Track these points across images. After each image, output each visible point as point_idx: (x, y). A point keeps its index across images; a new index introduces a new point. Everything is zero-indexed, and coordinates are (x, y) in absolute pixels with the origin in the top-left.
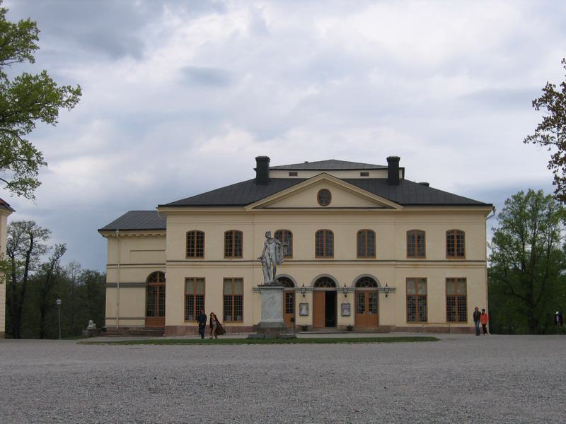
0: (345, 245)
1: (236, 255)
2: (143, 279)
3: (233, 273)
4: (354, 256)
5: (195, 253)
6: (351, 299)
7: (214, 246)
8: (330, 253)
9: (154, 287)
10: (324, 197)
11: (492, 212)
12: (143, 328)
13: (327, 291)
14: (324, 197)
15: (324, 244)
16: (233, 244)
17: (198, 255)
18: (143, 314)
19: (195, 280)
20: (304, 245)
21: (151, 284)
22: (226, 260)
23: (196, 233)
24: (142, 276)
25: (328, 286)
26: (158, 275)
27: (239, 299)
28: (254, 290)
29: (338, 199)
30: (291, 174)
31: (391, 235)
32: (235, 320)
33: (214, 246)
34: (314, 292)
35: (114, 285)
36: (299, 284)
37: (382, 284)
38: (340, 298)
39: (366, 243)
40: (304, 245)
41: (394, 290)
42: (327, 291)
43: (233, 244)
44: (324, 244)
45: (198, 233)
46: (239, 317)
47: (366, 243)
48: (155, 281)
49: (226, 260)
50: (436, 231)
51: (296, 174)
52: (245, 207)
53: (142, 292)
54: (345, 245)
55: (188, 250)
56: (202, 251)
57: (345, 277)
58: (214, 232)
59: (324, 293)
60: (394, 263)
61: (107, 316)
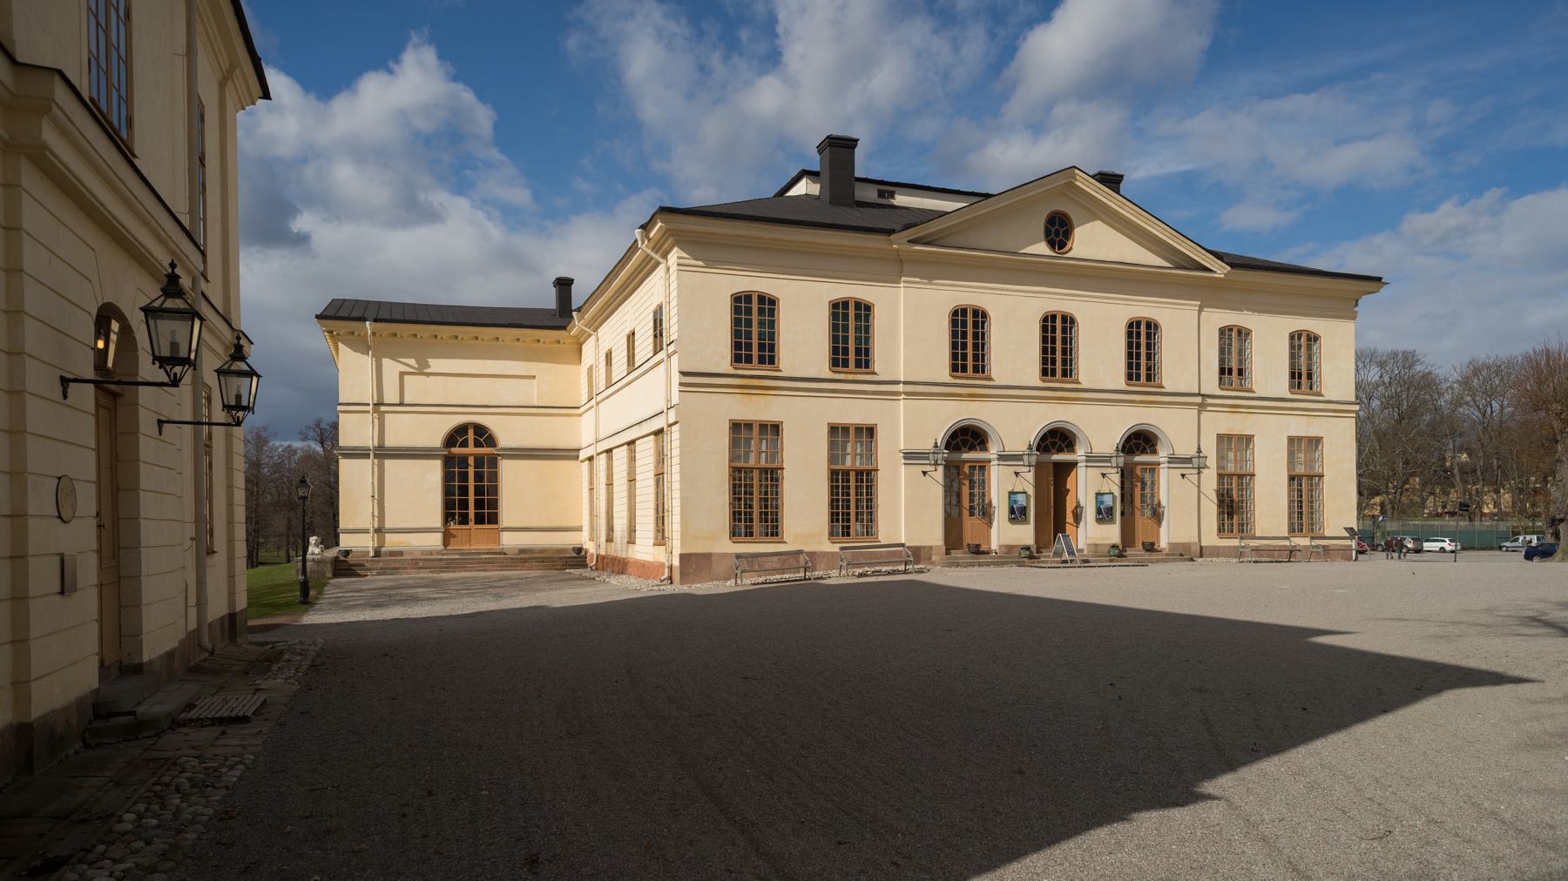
1: (858, 365)
2: (436, 440)
3: (853, 412)
5: (755, 353)
6: (1113, 484)
7: (803, 339)
9: (463, 461)
12: (439, 553)
15: (1057, 344)
16: (851, 339)
17: (762, 360)
18: (437, 522)
20: (1013, 350)
21: (456, 450)
22: (837, 376)
24: (433, 432)
26: (471, 432)
27: (866, 478)
28: (911, 456)
30: (881, 194)
33: (803, 339)
35: (358, 453)
40: (1013, 350)
44: (1057, 344)
45: (762, 298)
48: (464, 444)
51: (892, 195)
52: (893, 237)
53: (433, 472)
55: (737, 346)
56: (772, 348)
57: (1101, 429)
61: (342, 525)
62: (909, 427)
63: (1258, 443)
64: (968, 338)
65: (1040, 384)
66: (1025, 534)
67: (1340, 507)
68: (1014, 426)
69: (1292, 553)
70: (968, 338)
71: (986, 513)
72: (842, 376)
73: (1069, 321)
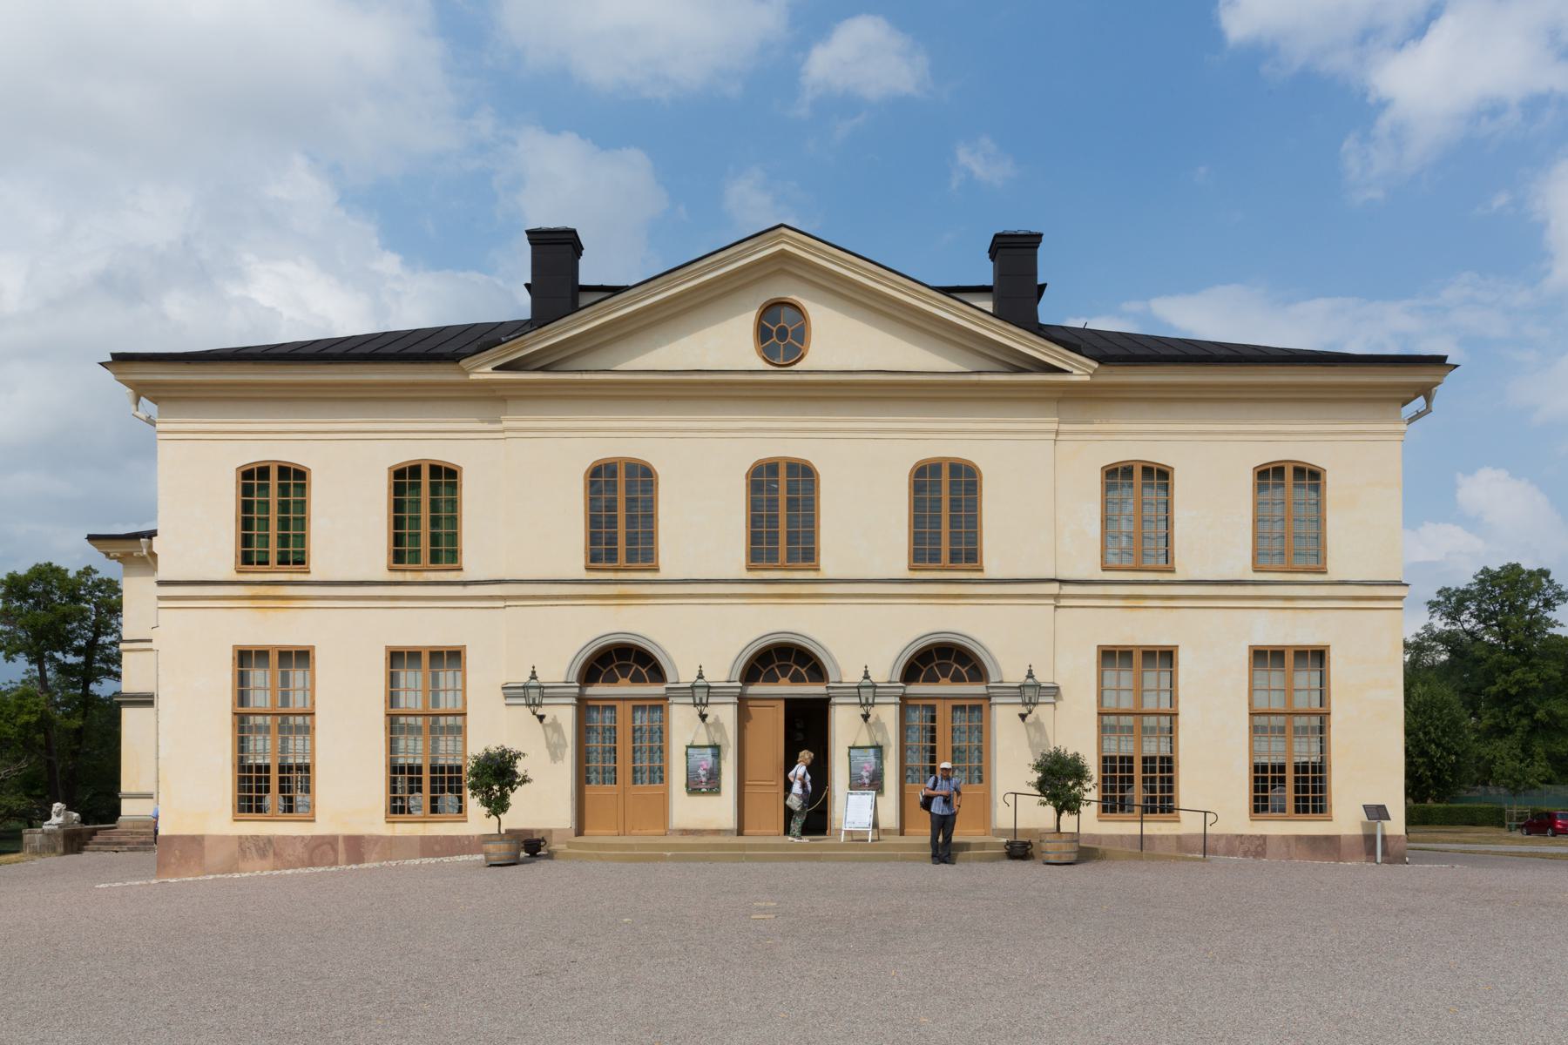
0: (864, 516)
1: (435, 557)
3: (424, 626)
4: (899, 564)
7: (348, 523)
8: (805, 550)
10: (780, 331)
11: (1420, 403)
13: (791, 696)
14: (780, 331)
15: (782, 513)
17: (283, 561)
19: (274, 658)
20: (702, 519)
22: (398, 576)
23: (274, 474)
25: (796, 679)
28: (509, 691)
29: (839, 341)
31: (1041, 479)
32: (434, 810)
33: (348, 523)
34: (743, 704)
36: (682, 671)
37: (1007, 666)
38: (844, 726)
39: (945, 512)
40: (702, 519)
41: (1055, 691)
42: (791, 696)
43: (424, 511)
44: (782, 513)
46: (449, 798)
47: (945, 512)
49: (398, 576)
50: (1213, 462)
54: (864, 516)
57: (863, 642)
58: (349, 466)
59: (781, 706)
60: (1054, 588)
62: (515, 651)
63: (1184, 659)
64: (620, 514)
65: (905, 573)
66: (719, 811)
67: (1369, 764)
68: (703, 641)
69: (1258, 847)
70: (620, 514)
71: (659, 775)
72: (409, 577)
73: (803, 475)
